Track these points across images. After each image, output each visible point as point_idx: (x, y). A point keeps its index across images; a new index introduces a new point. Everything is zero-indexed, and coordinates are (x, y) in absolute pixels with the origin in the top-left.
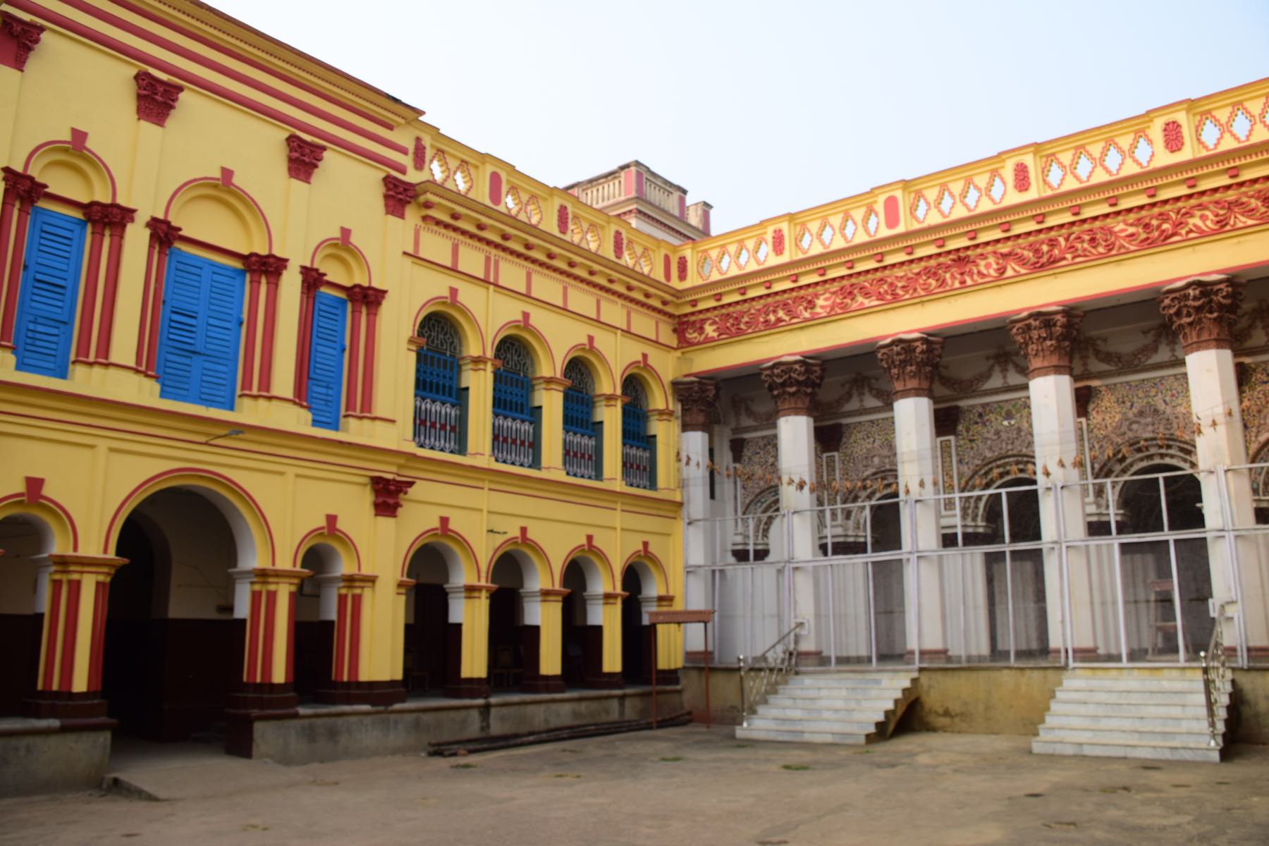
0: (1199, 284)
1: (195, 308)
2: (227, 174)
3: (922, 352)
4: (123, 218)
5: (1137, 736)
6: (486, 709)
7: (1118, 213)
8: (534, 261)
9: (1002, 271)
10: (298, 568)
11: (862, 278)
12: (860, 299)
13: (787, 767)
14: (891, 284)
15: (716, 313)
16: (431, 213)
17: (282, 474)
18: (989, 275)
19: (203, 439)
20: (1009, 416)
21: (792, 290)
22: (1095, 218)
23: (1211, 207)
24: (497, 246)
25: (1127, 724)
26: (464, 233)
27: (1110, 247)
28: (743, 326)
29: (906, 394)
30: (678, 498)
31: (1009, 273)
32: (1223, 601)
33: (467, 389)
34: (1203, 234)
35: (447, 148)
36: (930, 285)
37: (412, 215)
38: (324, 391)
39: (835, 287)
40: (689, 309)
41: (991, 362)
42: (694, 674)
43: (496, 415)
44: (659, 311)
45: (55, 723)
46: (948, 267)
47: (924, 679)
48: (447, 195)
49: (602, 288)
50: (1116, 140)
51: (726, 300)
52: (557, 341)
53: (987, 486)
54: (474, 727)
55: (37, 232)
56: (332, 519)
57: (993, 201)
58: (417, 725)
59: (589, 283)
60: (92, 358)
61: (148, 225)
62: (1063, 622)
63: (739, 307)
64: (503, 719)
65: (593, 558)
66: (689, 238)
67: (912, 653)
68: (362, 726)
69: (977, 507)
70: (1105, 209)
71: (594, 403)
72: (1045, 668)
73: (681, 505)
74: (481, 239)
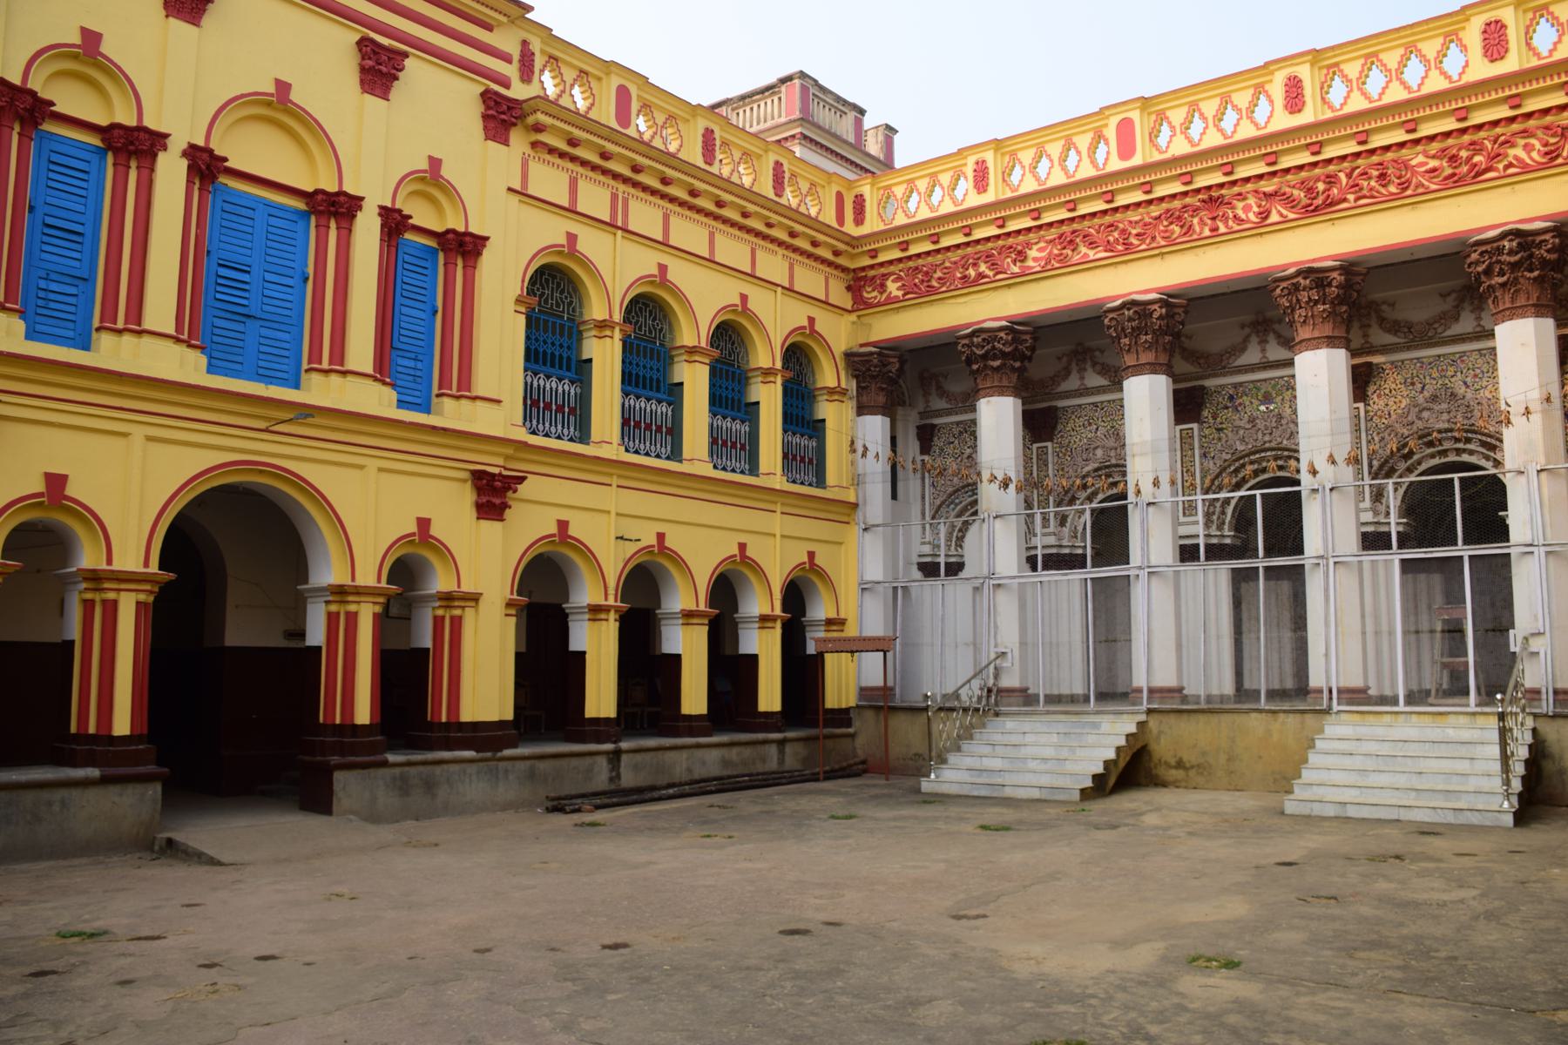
0: (1517, 233)
1: (247, 261)
2: (283, 88)
3: (1161, 317)
4: (153, 145)
5: (1414, 794)
6: (617, 753)
7: (1417, 142)
8: (672, 200)
9: (1264, 215)
10: (384, 584)
11: (1086, 223)
12: (1083, 250)
13: (984, 827)
14: (1123, 231)
15: (901, 266)
16: (543, 137)
17: (361, 467)
18: (1249, 221)
19: (262, 425)
20: (1267, 399)
21: (998, 237)
22: (1387, 148)
23: (1540, 133)
24: (626, 180)
25: (1402, 781)
26: (584, 163)
27: (1404, 186)
28: (935, 283)
29: (1138, 370)
30: (852, 499)
31: (1274, 217)
32: (1526, 634)
33: (590, 360)
34: (1526, 169)
35: (561, 53)
36: (1173, 232)
37: (519, 140)
38: (411, 364)
39: (1053, 233)
40: (867, 262)
41: (1247, 330)
42: (870, 714)
43: (626, 394)
44: (830, 264)
45: (94, 772)
46: (1196, 210)
47: (1154, 723)
48: (564, 115)
49: (758, 234)
50: (1420, 46)
51: (914, 250)
52: (702, 300)
53: (1237, 487)
54: (601, 777)
55: (44, 163)
56: (424, 524)
57: (1256, 125)
58: (532, 775)
59: (741, 228)
60: (120, 324)
61: (185, 154)
62: (1326, 655)
63: (930, 259)
64: (636, 768)
65: (747, 572)
66: (867, 171)
67: (1140, 691)
68: (464, 775)
69: (1223, 513)
70: (1400, 136)
71: (747, 379)
72: (1303, 712)
73: (855, 506)
74: (605, 172)
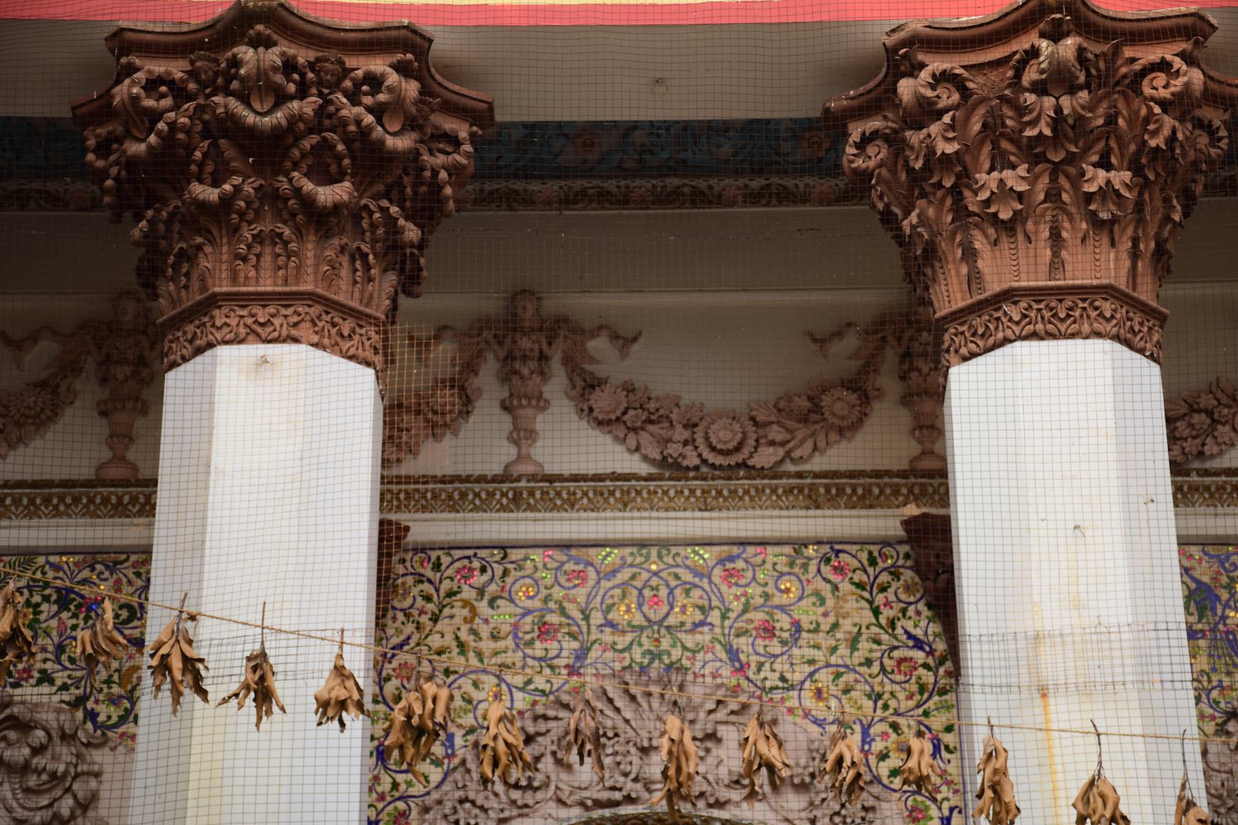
3: (1180, 105)
29: (1055, 312)
